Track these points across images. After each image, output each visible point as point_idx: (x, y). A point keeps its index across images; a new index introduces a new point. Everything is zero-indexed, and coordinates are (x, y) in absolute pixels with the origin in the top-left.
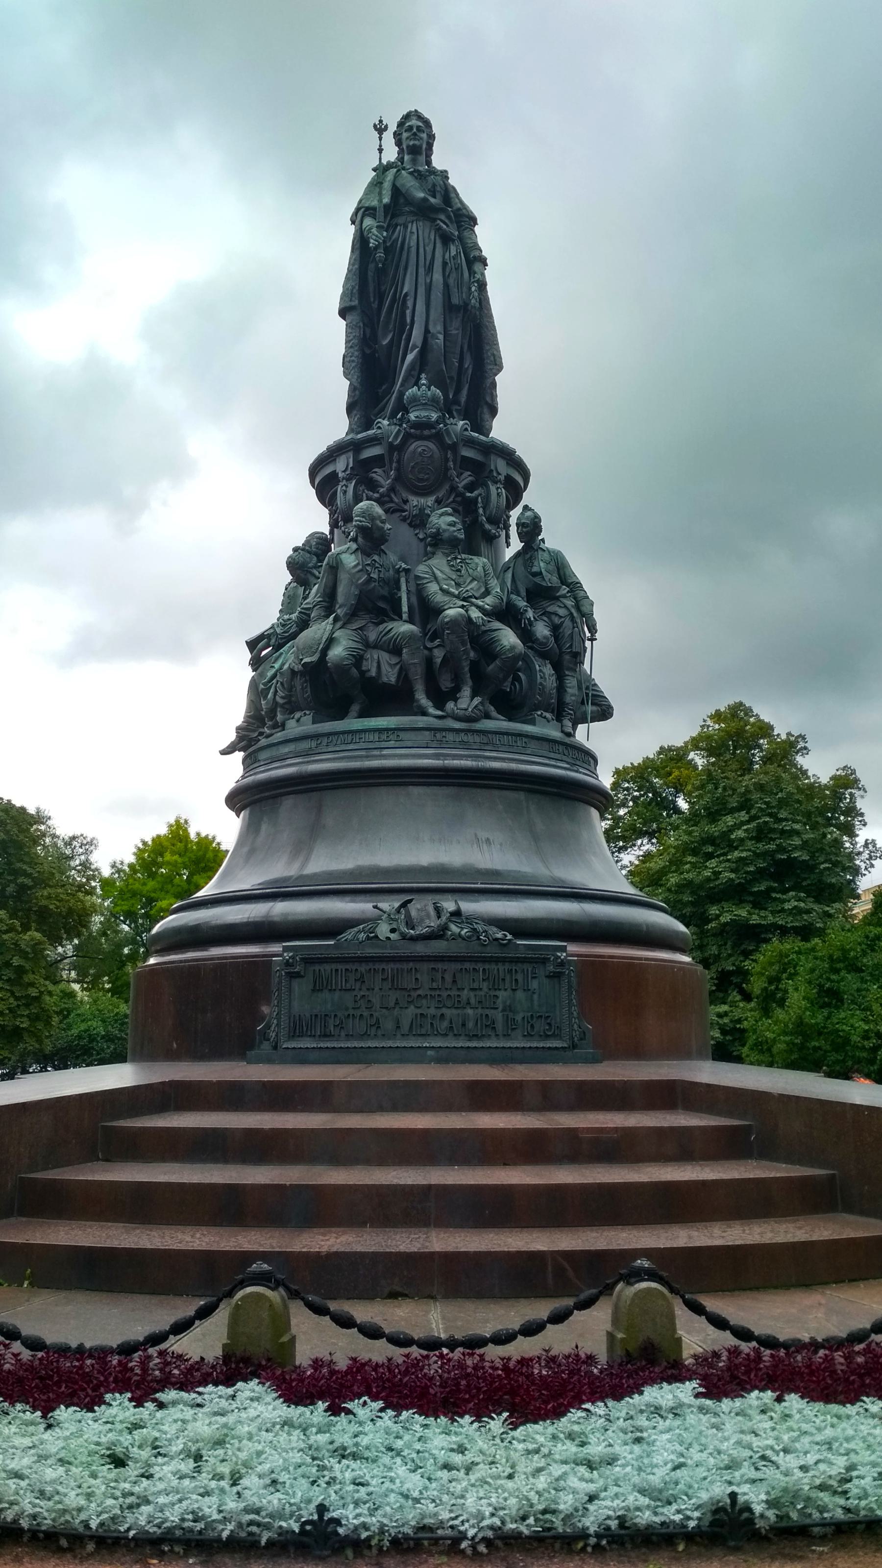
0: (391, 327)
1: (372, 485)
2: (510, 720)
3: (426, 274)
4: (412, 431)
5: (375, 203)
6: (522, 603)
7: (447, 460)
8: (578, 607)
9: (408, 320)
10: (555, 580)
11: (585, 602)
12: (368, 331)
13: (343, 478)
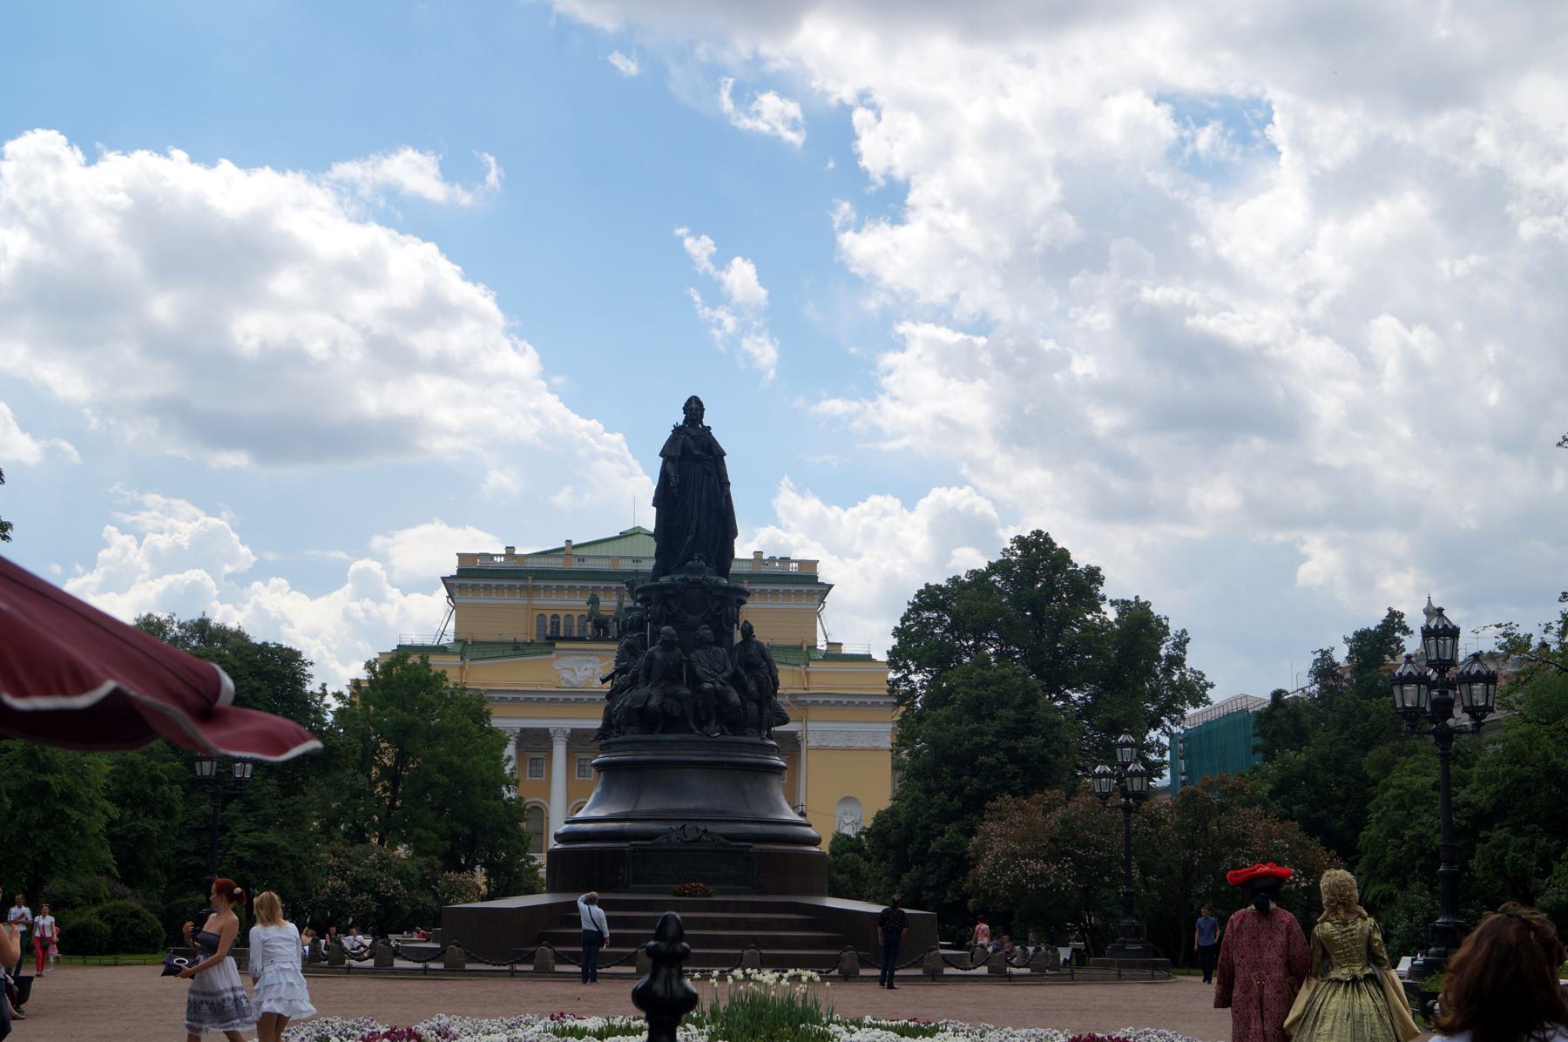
2: (735, 735)
5: (673, 454)
10: (760, 659)
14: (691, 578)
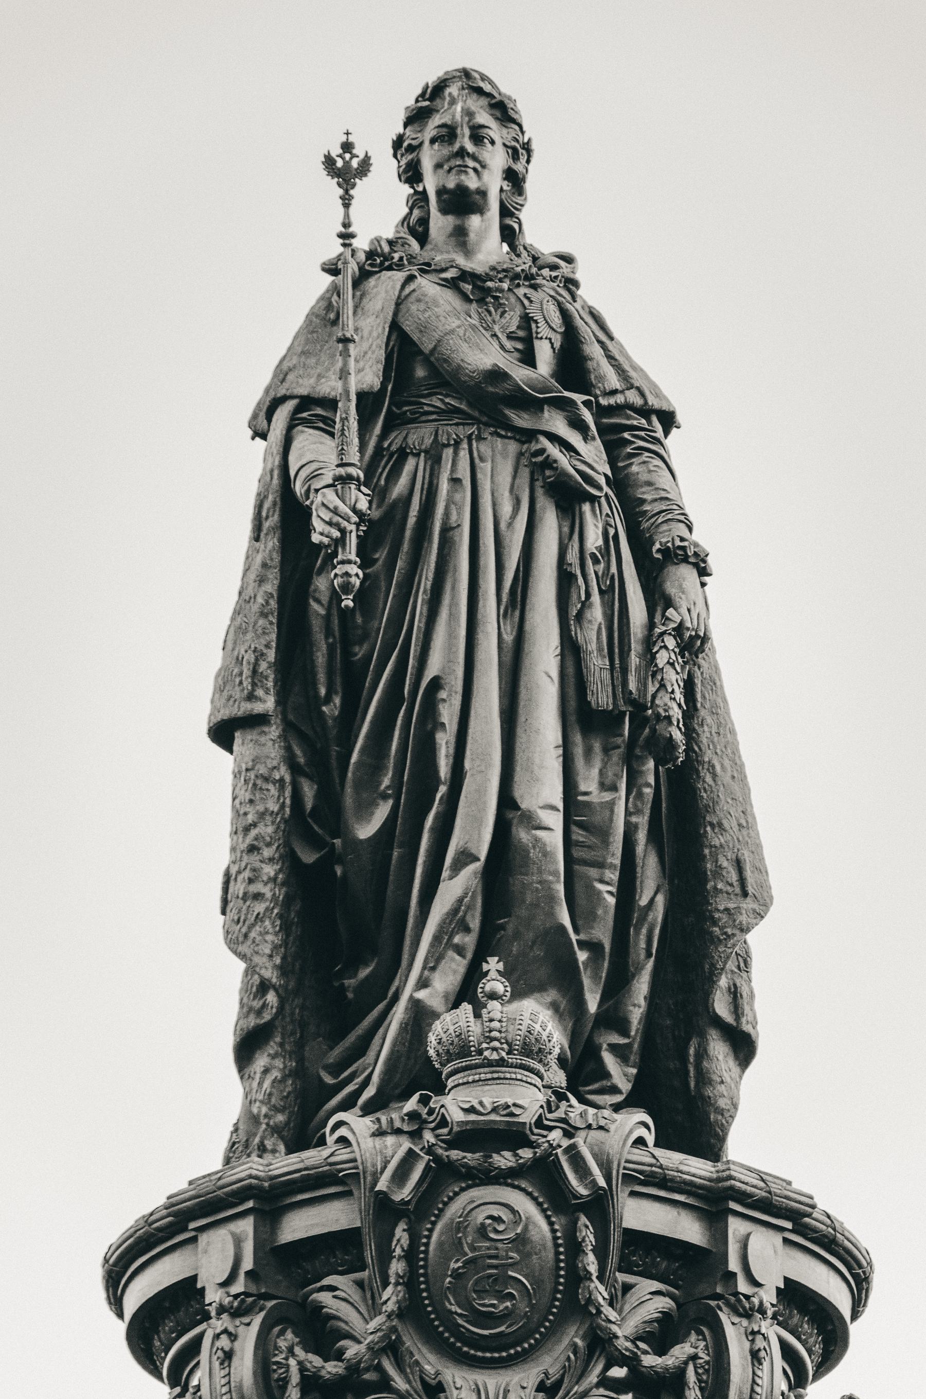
0: (386, 782)
3: (503, 616)
4: (455, 1154)
7: (575, 1248)
9: (444, 768)
12: (309, 791)
13: (221, 1310)
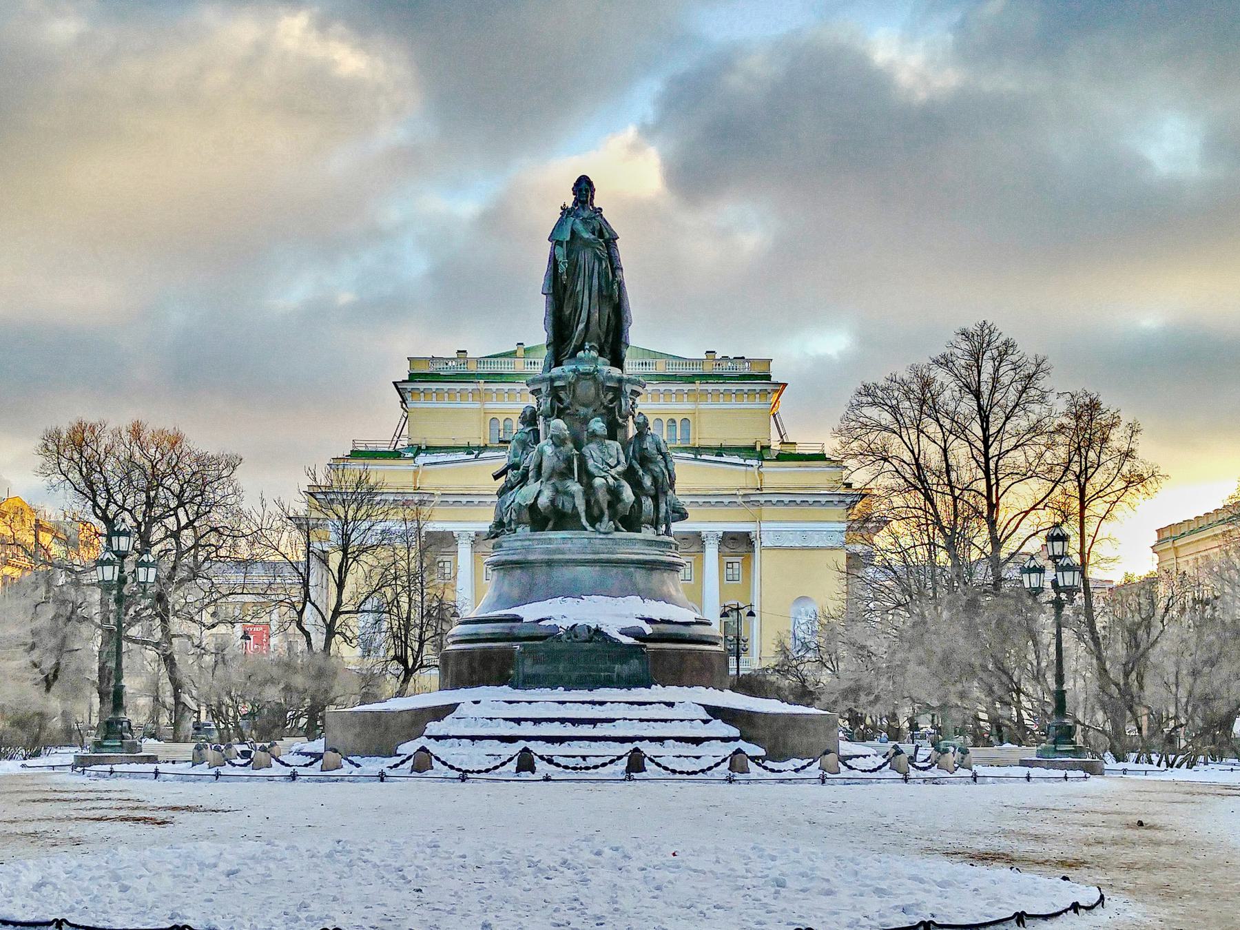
1: (560, 400)
6: (637, 466)
8: (666, 467)
10: (655, 452)
11: (669, 464)
14: (581, 368)
